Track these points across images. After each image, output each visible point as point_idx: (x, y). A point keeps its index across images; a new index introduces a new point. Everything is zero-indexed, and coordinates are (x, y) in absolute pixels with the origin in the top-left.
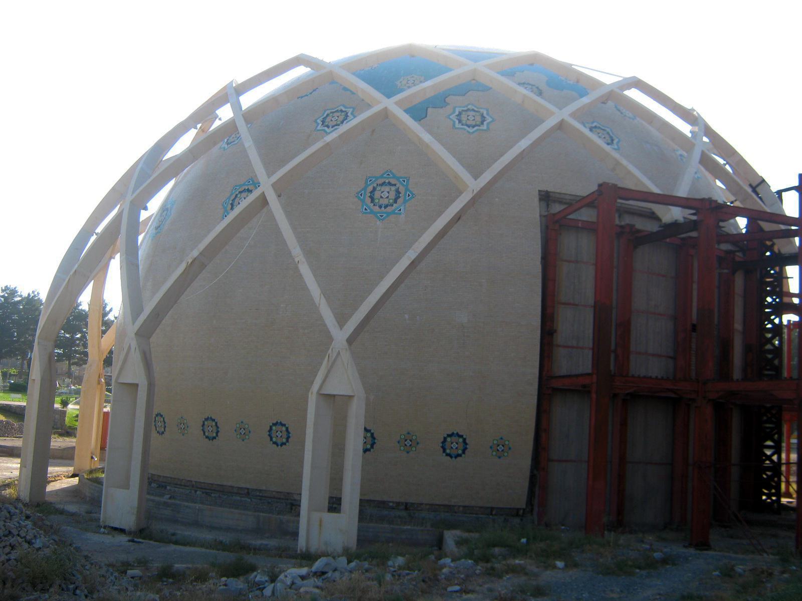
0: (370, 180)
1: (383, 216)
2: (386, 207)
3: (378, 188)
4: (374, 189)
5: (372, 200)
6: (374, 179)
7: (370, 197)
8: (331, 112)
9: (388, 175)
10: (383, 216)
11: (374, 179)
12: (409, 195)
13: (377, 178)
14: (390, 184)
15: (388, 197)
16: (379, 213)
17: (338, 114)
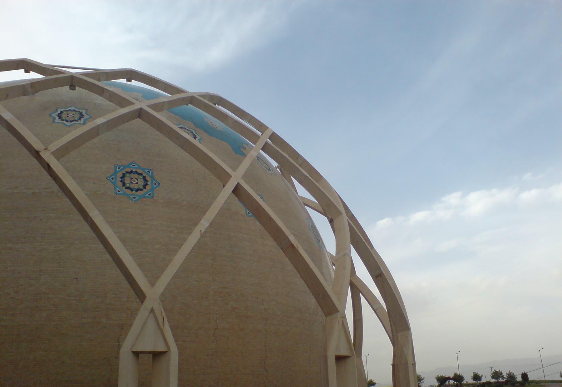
0: (119, 168)
1: (135, 198)
2: (137, 191)
3: (128, 175)
4: (124, 176)
5: (124, 184)
6: (137, 167)
7: (121, 181)
8: (64, 111)
9: (134, 165)
10: (135, 198)
11: (137, 167)
12: (155, 184)
13: (125, 167)
14: (136, 172)
15: (137, 183)
16: (132, 195)
17: (74, 113)
